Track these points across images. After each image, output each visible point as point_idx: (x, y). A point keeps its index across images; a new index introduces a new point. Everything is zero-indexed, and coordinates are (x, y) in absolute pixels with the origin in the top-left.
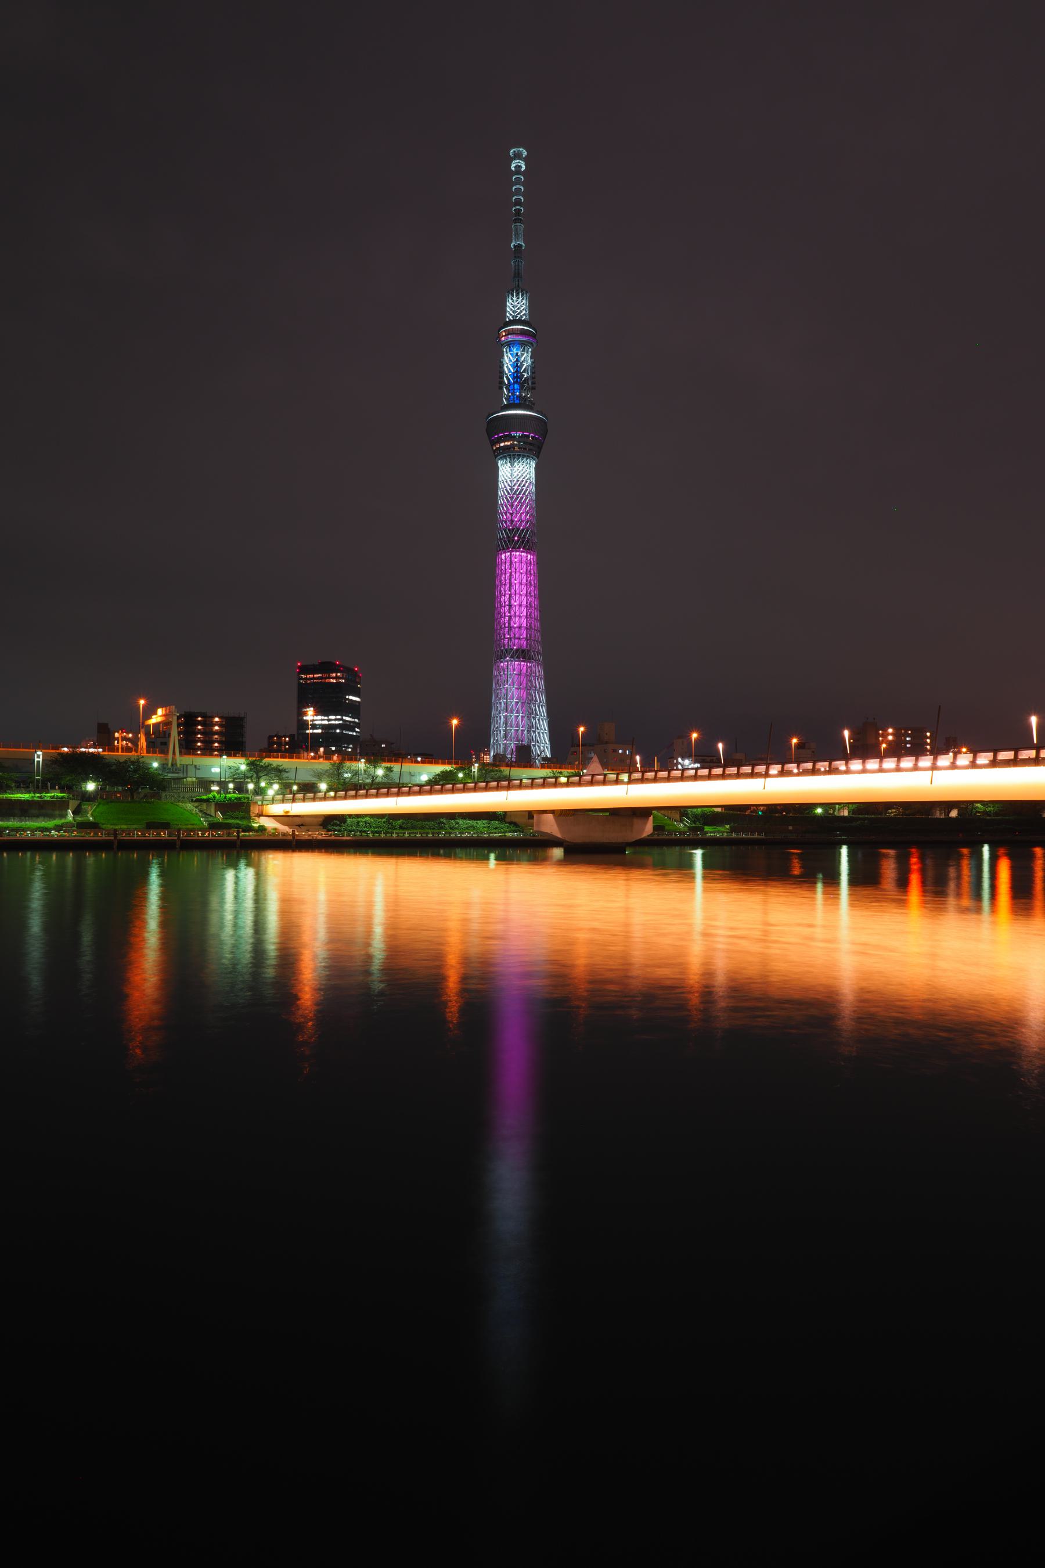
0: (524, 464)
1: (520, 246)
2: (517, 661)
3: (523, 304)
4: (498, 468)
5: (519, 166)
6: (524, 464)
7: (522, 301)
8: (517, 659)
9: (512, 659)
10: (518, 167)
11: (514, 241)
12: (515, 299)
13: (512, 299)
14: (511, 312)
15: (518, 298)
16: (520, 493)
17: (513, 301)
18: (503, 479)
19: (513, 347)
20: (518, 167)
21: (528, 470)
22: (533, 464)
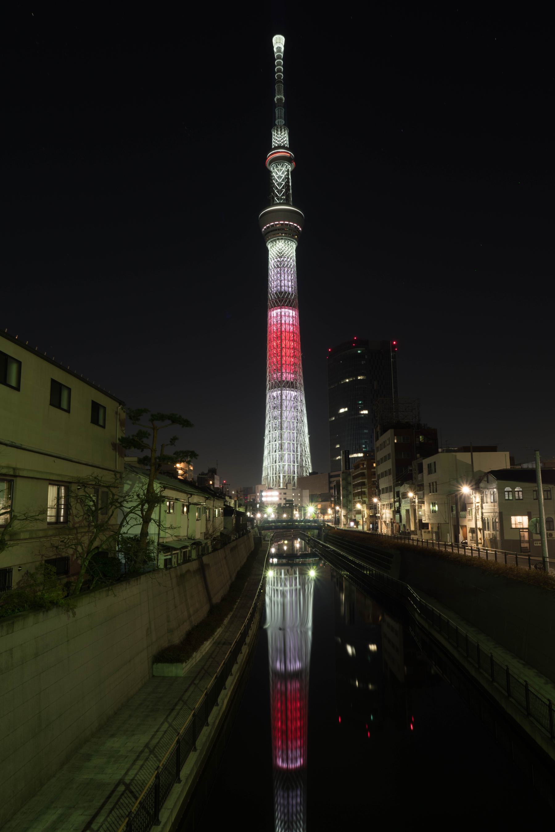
0: (289, 246)
1: (281, 99)
2: (288, 390)
3: (285, 137)
4: (266, 251)
5: (280, 48)
6: (289, 246)
7: (284, 135)
8: (287, 389)
9: (284, 388)
10: (279, 49)
11: (276, 94)
12: (279, 133)
13: (277, 133)
14: (276, 141)
15: (282, 132)
16: (286, 266)
17: (278, 135)
18: (273, 256)
19: (278, 164)
20: (279, 49)
21: (292, 251)
22: (295, 246)
